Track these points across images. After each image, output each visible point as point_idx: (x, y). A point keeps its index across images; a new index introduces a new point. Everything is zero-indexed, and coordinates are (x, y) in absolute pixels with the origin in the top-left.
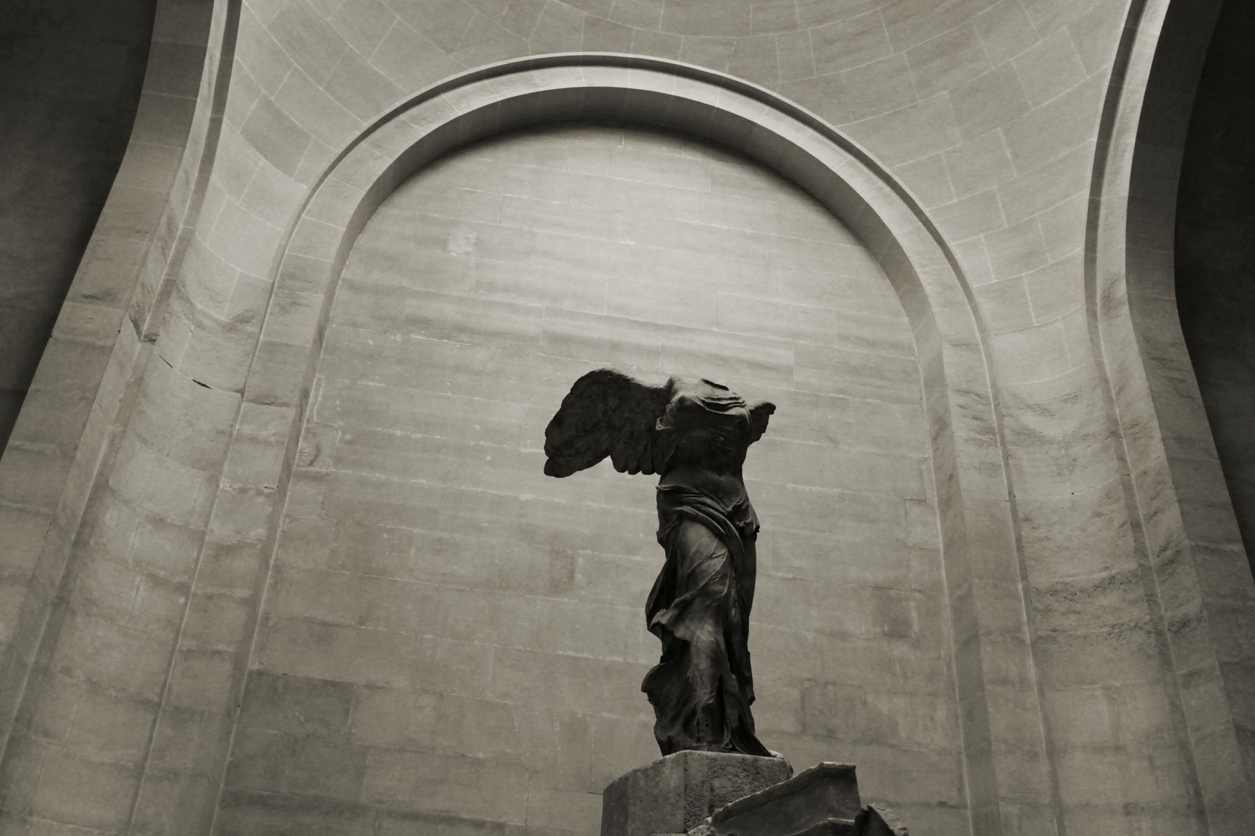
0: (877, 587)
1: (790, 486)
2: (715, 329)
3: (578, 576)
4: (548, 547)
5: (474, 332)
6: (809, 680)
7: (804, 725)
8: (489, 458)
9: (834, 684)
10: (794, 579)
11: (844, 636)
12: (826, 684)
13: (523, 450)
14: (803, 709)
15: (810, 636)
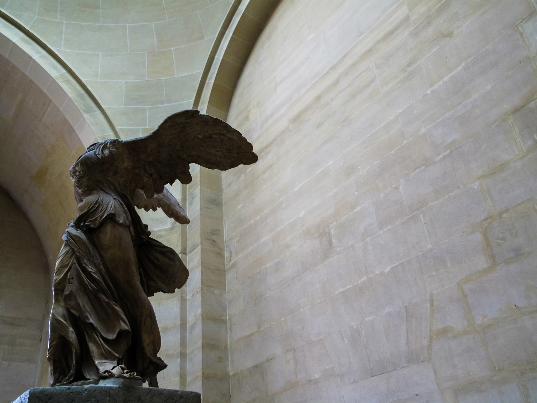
0: (516, 110)
1: (429, 92)
2: (360, 38)
3: (334, 241)
4: (317, 235)
5: (266, 147)
6: (485, 220)
7: (493, 257)
8: (284, 206)
9: (507, 210)
10: (451, 152)
11: (503, 167)
12: (500, 215)
13: (296, 189)
14: (488, 245)
15: (476, 185)
